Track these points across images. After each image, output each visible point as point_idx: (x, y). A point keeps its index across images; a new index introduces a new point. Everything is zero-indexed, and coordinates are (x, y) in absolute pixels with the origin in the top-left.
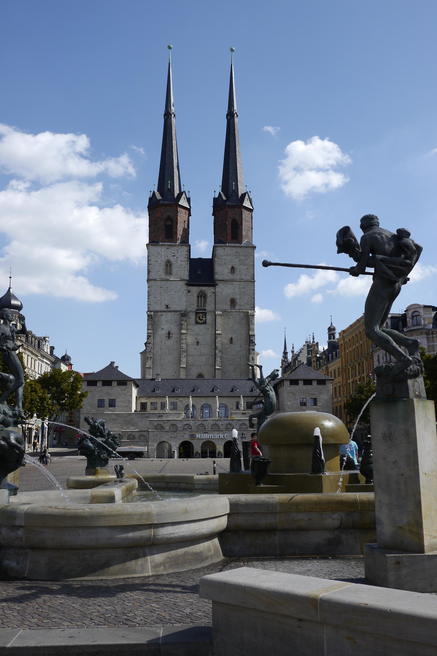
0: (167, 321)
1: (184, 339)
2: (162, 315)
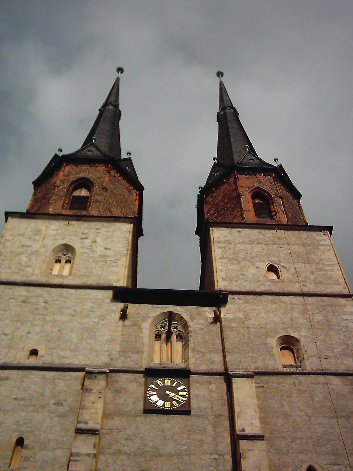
0: (22, 399)
1: (88, 455)
2: (7, 379)
